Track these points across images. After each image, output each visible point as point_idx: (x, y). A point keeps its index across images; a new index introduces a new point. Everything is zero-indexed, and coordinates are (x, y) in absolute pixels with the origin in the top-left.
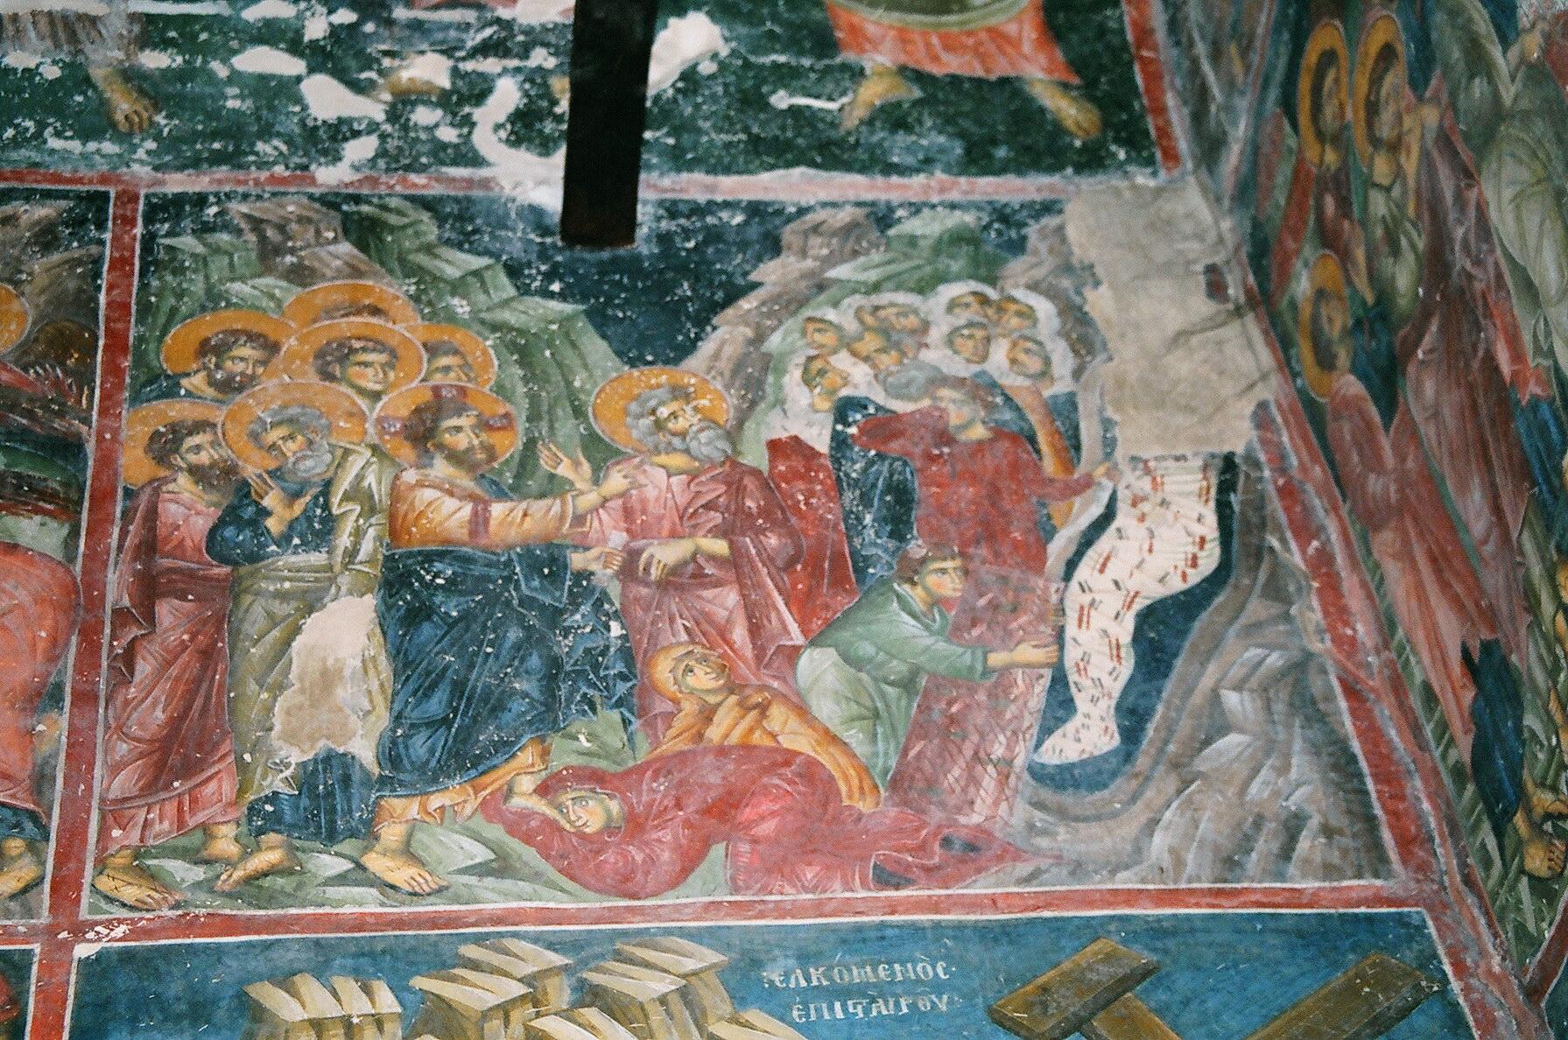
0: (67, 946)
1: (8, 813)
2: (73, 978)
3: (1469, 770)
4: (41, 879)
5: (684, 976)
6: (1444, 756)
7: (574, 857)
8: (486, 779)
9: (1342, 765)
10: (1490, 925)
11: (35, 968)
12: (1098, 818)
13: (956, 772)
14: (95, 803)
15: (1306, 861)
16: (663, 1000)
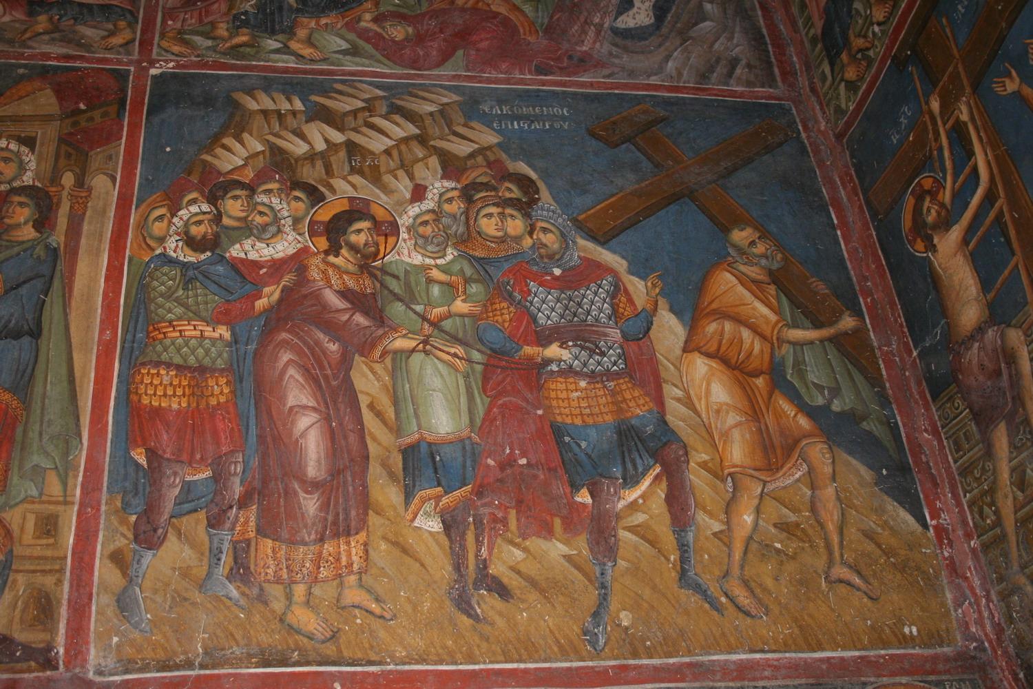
0: (147, 69)
1: (119, 10)
2: (149, 83)
3: (820, 37)
4: (133, 40)
5: (442, 105)
6: (807, 34)
7: (391, 50)
8: (348, 13)
9: (757, 40)
10: (822, 109)
11: (131, 77)
12: (643, 53)
13: (576, 28)
14: (160, 9)
15: (739, 78)
16: (431, 114)
